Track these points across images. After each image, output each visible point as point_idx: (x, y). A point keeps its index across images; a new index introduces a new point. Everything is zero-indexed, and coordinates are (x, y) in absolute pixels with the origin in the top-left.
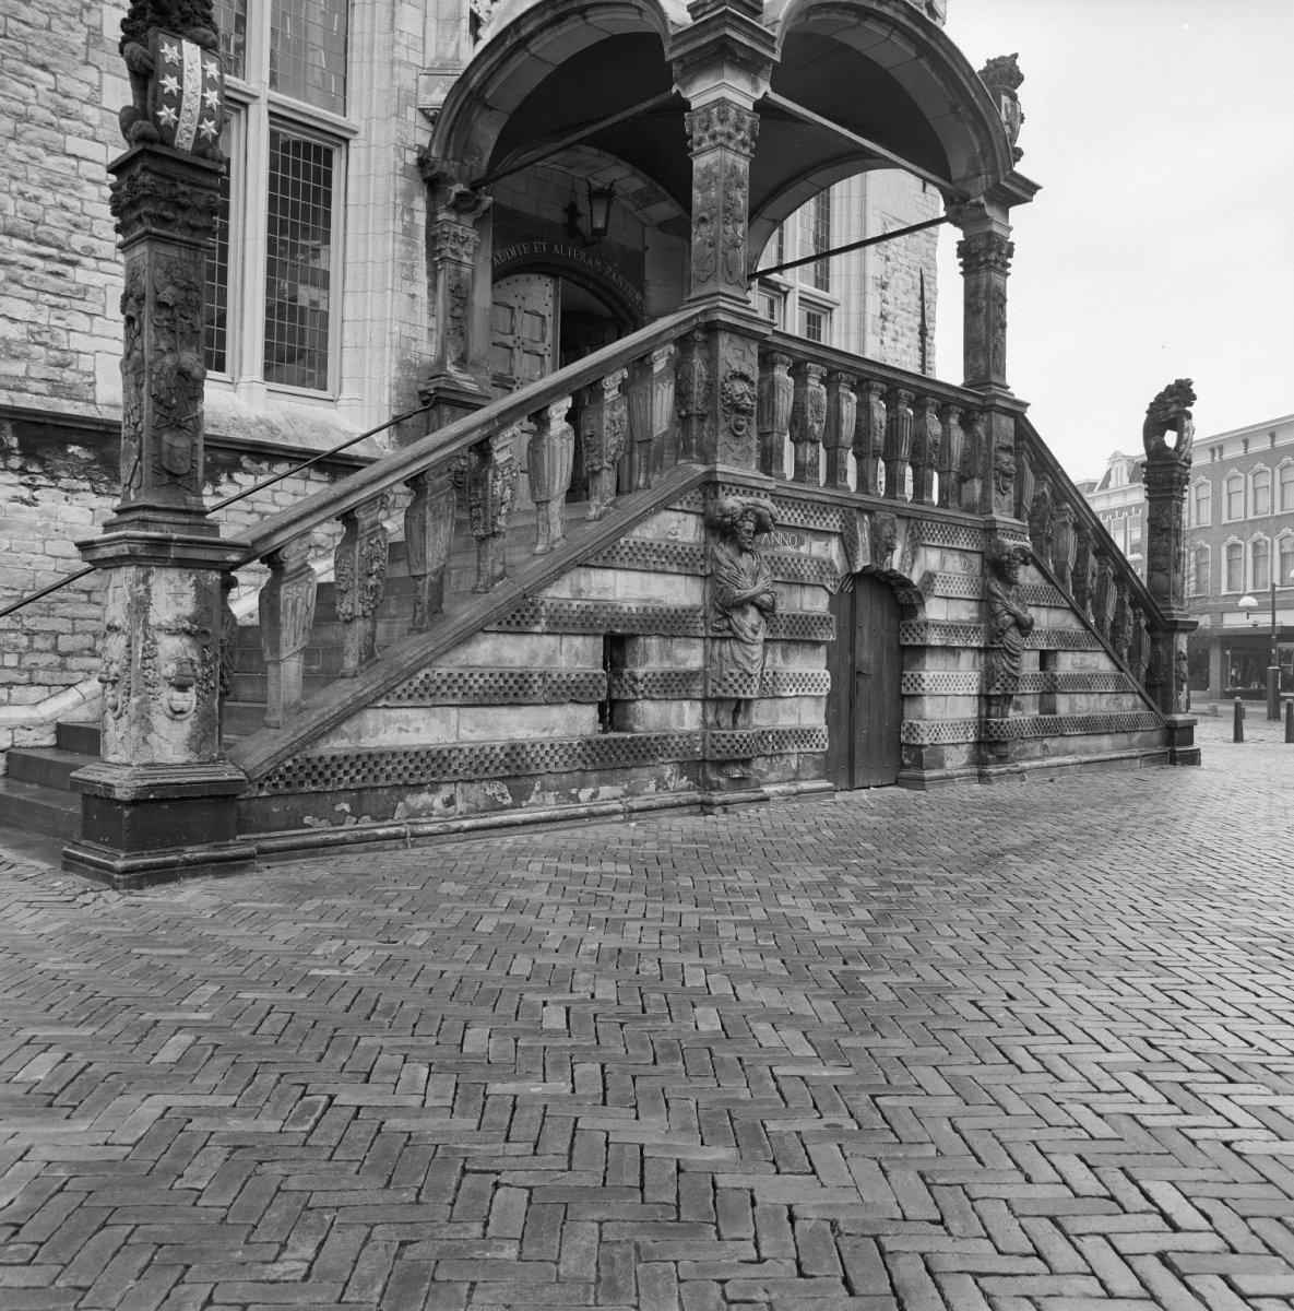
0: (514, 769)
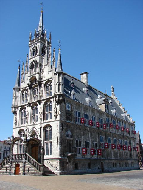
0: (3, 172)
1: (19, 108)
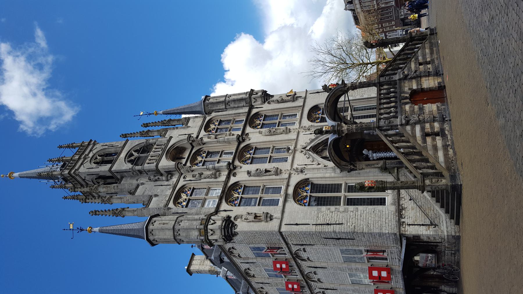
0: (445, 147)
1: (224, 206)
